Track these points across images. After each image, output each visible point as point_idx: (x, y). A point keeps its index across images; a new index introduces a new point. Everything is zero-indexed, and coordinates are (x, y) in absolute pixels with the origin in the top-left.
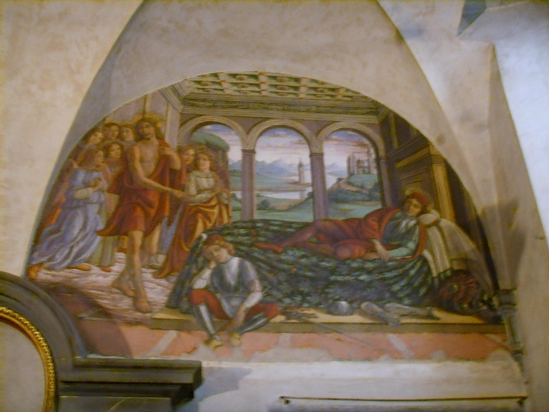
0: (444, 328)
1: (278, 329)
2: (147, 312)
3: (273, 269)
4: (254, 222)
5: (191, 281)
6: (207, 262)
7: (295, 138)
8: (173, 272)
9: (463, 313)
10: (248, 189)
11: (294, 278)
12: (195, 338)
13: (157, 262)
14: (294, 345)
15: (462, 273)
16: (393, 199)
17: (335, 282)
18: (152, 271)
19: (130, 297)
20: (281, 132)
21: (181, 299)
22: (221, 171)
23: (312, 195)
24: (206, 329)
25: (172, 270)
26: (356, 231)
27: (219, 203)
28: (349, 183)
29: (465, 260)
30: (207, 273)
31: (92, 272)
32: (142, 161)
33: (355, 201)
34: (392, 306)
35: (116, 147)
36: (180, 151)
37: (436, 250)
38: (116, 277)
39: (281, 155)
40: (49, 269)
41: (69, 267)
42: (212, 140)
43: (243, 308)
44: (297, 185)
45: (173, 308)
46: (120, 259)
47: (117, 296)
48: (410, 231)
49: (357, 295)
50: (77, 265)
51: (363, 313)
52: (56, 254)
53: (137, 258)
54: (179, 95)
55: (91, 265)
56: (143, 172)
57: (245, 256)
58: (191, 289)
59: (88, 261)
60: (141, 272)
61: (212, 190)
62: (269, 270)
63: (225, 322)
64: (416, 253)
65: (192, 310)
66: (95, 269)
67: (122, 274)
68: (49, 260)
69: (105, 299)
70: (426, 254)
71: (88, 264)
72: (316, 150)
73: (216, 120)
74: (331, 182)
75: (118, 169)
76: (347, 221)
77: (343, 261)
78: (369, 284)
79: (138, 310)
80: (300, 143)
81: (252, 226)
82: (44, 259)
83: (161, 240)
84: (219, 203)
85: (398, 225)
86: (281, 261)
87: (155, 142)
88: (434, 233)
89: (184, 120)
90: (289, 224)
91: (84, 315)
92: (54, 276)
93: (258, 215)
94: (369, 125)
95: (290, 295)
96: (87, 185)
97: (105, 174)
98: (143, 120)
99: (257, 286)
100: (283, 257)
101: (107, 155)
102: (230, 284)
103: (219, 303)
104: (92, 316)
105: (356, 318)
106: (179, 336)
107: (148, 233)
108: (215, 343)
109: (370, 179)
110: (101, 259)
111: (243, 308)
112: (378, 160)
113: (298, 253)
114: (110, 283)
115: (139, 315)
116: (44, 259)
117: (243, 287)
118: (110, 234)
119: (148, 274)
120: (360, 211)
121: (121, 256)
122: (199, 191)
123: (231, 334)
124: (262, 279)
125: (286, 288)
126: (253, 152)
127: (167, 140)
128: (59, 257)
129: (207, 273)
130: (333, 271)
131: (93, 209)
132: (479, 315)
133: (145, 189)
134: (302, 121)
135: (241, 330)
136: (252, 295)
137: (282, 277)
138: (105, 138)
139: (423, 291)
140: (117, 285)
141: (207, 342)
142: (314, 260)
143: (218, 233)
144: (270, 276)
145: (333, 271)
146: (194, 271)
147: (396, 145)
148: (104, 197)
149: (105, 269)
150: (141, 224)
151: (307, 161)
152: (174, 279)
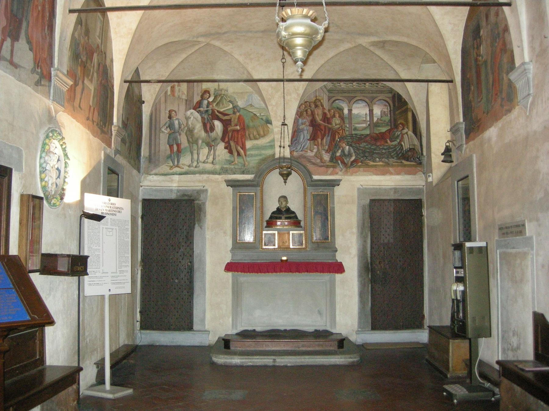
0: (405, 166)
1: (360, 167)
3: (358, 149)
4: (352, 134)
6: (340, 148)
7: (364, 104)
9: (411, 161)
10: (350, 123)
11: (364, 152)
14: (364, 171)
15: (412, 150)
16: (394, 125)
17: (376, 153)
20: (360, 102)
21: (333, 159)
22: (342, 118)
23: (369, 125)
25: (330, 150)
26: (382, 137)
27: (342, 129)
28: (381, 120)
29: (414, 145)
30: (340, 151)
32: (318, 115)
33: (383, 126)
34: (391, 160)
35: (309, 110)
36: (329, 111)
37: (406, 142)
39: (360, 110)
40: (297, 152)
42: (339, 106)
44: (365, 121)
48: (398, 136)
49: (381, 156)
51: (383, 162)
53: (320, 147)
54: (327, 89)
56: (319, 118)
57: (351, 145)
59: (307, 149)
61: (339, 124)
62: (357, 149)
64: (400, 144)
66: (309, 151)
67: (316, 153)
70: (403, 143)
72: (371, 108)
73: (339, 98)
74: (375, 119)
75: (311, 118)
76: (380, 133)
77: (378, 146)
78: (385, 153)
79: (322, 163)
80: (366, 106)
81: (351, 136)
83: (326, 141)
84: (342, 129)
85: (395, 134)
86: (360, 146)
87: (321, 108)
88: (405, 136)
89: (329, 98)
90: (362, 135)
93: (353, 132)
94: (388, 97)
95: (363, 157)
96: (302, 124)
97: (307, 120)
98: (316, 99)
99: (354, 154)
100: (361, 145)
101: (307, 113)
105: (381, 163)
107: (322, 139)
108: (343, 171)
109: (387, 118)
112: (390, 111)
113: (365, 144)
117: (350, 155)
118: (312, 140)
119: (324, 152)
120: (384, 130)
121: (315, 147)
122: (336, 125)
123: (347, 168)
124: (355, 152)
125: (362, 155)
126: (351, 110)
127: (325, 107)
128: (299, 148)
129: (340, 151)
130: (375, 150)
131: (305, 132)
132: (416, 162)
133: (319, 125)
134: (367, 97)
137: (361, 151)
138: (306, 107)
139: (400, 155)
140: (316, 155)
141: (341, 171)
142: (370, 146)
143: (342, 138)
144: (357, 152)
145: (375, 150)
147: (397, 105)
148: (308, 128)
149: (312, 151)
150: (320, 137)
151: (368, 113)
152: (331, 153)
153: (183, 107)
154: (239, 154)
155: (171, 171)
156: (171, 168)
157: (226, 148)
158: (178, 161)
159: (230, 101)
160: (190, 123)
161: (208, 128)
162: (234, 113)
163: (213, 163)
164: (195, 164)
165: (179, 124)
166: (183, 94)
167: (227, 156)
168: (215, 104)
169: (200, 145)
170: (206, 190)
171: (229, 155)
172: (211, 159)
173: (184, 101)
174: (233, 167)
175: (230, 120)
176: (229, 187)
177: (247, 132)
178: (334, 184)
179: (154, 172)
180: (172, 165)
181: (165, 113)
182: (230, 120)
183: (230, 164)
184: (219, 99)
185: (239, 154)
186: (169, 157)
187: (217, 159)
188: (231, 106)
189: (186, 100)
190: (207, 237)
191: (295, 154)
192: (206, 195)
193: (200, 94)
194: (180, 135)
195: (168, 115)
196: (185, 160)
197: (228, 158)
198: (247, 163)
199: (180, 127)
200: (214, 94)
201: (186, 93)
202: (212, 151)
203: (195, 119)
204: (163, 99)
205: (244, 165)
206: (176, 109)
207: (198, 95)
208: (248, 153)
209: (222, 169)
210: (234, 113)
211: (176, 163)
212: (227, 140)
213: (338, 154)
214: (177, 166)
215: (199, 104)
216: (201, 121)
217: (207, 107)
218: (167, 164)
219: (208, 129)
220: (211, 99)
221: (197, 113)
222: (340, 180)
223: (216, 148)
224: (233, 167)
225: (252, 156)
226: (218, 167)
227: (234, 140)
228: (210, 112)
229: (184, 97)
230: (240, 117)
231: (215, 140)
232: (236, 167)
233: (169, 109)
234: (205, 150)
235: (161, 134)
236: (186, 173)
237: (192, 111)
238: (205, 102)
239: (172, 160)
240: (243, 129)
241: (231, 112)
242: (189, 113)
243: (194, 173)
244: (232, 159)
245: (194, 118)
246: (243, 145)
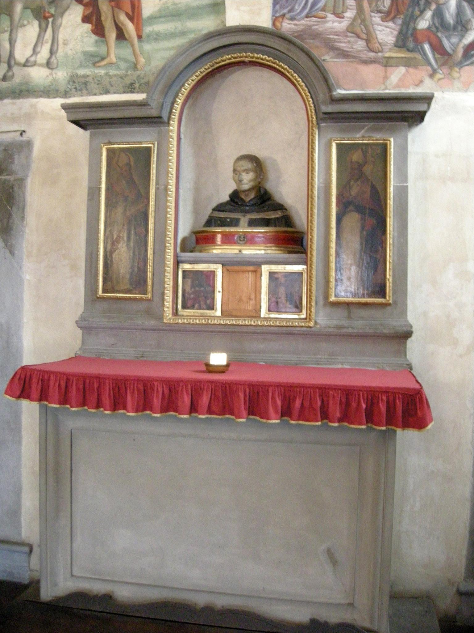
2: (379, 52)
5: (414, 23)
6: (428, 4)
8: (398, 15)
12: (423, 72)
13: (384, 6)
18: (380, 15)
19: (363, 39)
21: (407, 39)
24: (430, 64)
25: (398, 12)
30: (429, 14)
31: (328, 19)
38: (350, 22)
40: (292, 19)
41: (307, 17)
43: (462, 45)
45: (400, 47)
46: (351, 5)
47: (352, 39)
50: (314, 14)
52: (295, 5)
55: (327, 14)
58: (415, 29)
59: (323, 9)
60: (371, 16)
63: (446, 57)
65: (418, 48)
66: (330, 17)
67: (354, 20)
68: (289, 11)
69: (341, 42)
71: (324, 13)
79: (371, 50)
82: (285, 11)
91: (326, 57)
92: (295, 25)
102: (450, 24)
103: (440, 42)
104: (332, 58)
106: (407, 71)
108: (438, 76)
110: (335, 6)
111: (462, 45)
114: (345, 28)
115: (372, 55)
116: (285, 11)
119: (377, 18)
123: (451, 68)
128: (298, 8)
129: (429, 14)
135: (460, 64)
136: (469, 32)
140: (351, 29)
141: (431, 76)
146: (417, 12)
149: (339, 16)
152: (399, 21)
154: (121, 35)
157: (86, 19)
163: (48, 65)
169: (17, 17)
170: (29, 144)
171: (94, 37)
172: (44, 53)
174: (102, 72)
178: (407, 113)
183: (94, 64)
185: (121, 35)
187: (60, 53)
190: (27, 277)
191: (287, 26)
192: (28, 157)
197: (91, 49)
198: (142, 60)
205: (135, 67)
208: (147, 29)
209: (73, 79)
213: (423, 24)
222: (428, 99)
223: (59, 21)
224: (102, 72)
225: (157, 37)
226: (61, 75)
232: (112, 72)
234: (30, 31)
244: (103, 50)
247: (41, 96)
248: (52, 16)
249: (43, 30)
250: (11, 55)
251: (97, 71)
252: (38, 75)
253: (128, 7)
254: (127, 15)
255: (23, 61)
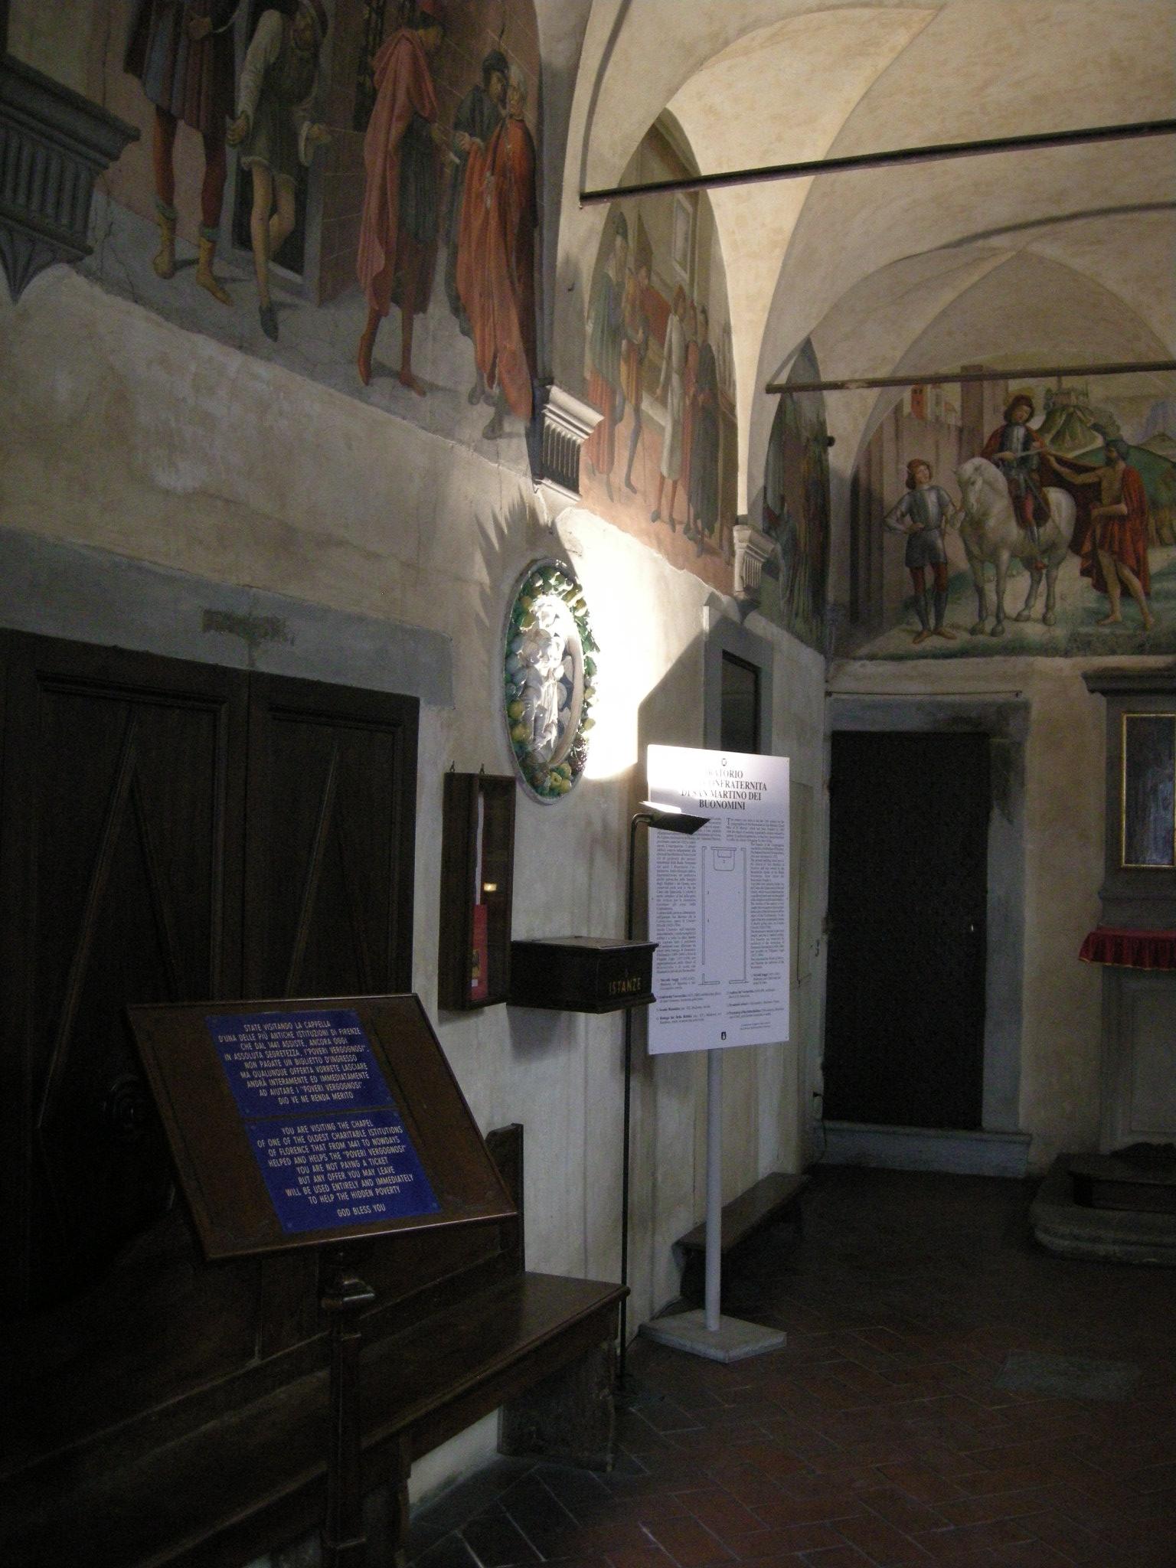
153: (949, 452)
154: (1126, 593)
155: (918, 648)
156: (918, 636)
157: (1085, 572)
158: (939, 616)
159: (1096, 427)
160: (972, 499)
161: (1029, 510)
162: (1110, 462)
163: (1044, 620)
164: (990, 624)
165: (941, 504)
166: (950, 409)
167: (1091, 598)
168: (1048, 438)
169: (1003, 568)
170: (1026, 707)
171: (1094, 594)
173: (954, 434)
174: (1107, 631)
175: (1096, 487)
176: (1098, 695)
177: (1152, 521)
179: (864, 651)
180: (920, 628)
181: (898, 471)
182: (1096, 487)
183: (1098, 622)
184: (1061, 420)
185: (1126, 593)
186: (912, 604)
187: (1058, 607)
188: (1099, 442)
189: (961, 430)
190: (1029, 846)
192: (1026, 719)
193: (1003, 408)
194: (943, 535)
195: (906, 477)
196: (961, 613)
197: (1093, 605)
198: (1152, 620)
199: (942, 513)
200: (1046, 406)
201: (957, 405)
202: (1044, 582)
203: (987, 484)
204: (889, 432)
206: (928, 456)
207: (995, 410)
208: (1156, 587)
209: (1074, 638)
210: (1110, 462)
211: (932, 622)
212: (1087, 547)
214: (937, 632)
215: (1001, 439)
216: (1005, 492)
217: (1026, 445)
218: (904, 626)
219: (1030, 516)
220: (1035, 424)
221: (993, 469)
223: (1054, 573)
224: (1107, 631)
226: (1060, 633)
227: (1111, 546)
228: (1035, 462)
229: (954, 420)
230: (1126, 473)
231: (1051, 548)
232: (1119, 632)
233: (908, 460)
234: (1020, 584)
235: (887, 535)
236: (963, 653)
237: (978, 461)
238: (1019, 433)
239: (919, 613)
240: (1140, 511)
241: (1097, 461)
242: (968, 467)
243: (985, 652)
244: (1107, 606)
245: (985, 482)
246: (1138, 561)
247: (1038, 654)
248: (1045, 566)
249: (1035, 582)
250: (1000, 607)
251: (1101, 630)
252: (1033, 631)
253: (1132, 562)
254: (1133, 570)
255: (1014, 616)
